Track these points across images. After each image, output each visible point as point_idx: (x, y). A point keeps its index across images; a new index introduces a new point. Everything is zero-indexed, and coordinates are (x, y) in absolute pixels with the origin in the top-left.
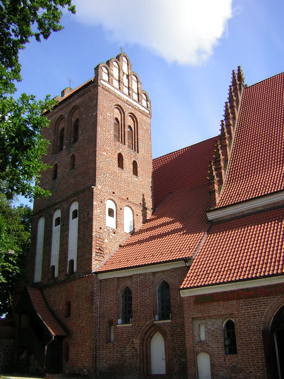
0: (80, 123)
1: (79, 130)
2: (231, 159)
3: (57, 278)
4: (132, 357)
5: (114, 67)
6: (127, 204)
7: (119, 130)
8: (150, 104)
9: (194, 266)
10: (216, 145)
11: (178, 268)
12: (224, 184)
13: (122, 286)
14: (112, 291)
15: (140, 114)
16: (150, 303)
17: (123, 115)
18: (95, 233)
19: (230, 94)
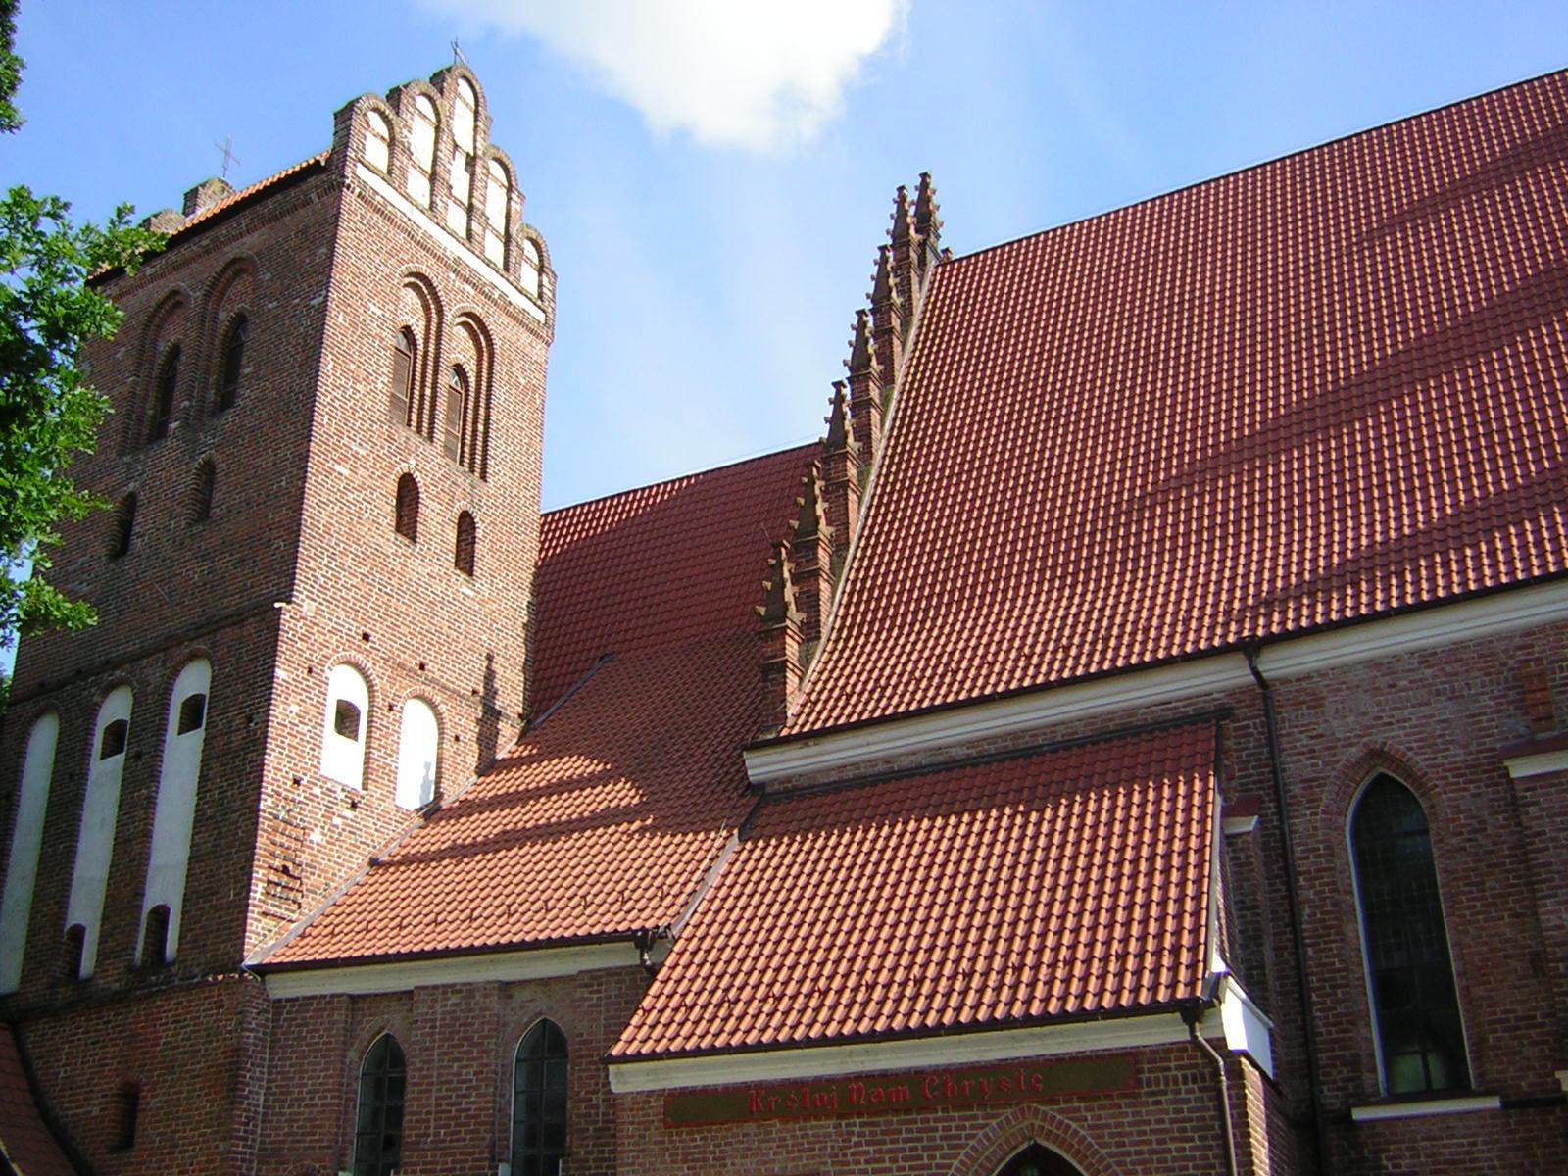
0: (252, 336)
1: (244, 360)
2: (860, 539)
3: (88, 980)
5: (416, 117)
6: (419, 688)
7: (413, 379)
8: (553, 284)
9: (673, 968)
10: (805, 480)
11: (609, 972)
12: (824, 639)
13: (370, 1029)
14: (321, 1050)
15: (506, 319)
16: (481, 1110)
17: (435, 320)
18: (270, 801)
19: (881, 279)
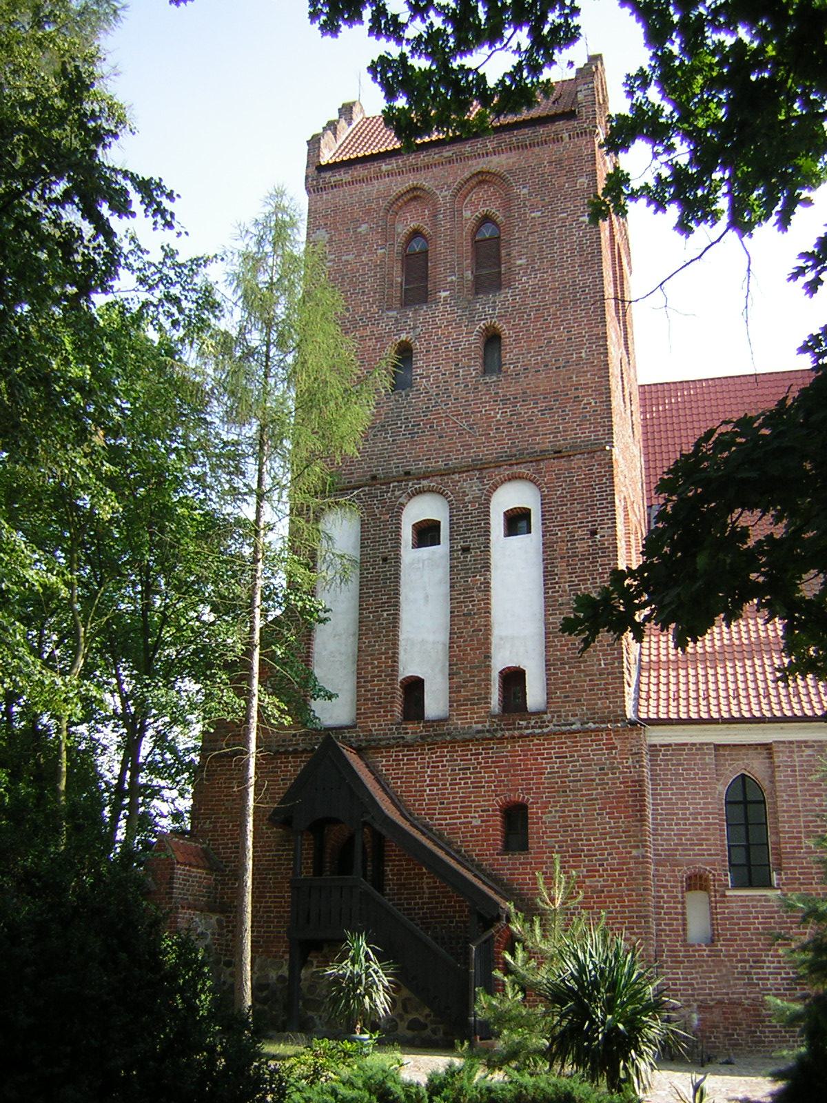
4: (785, 989)
14: (698, 784)
